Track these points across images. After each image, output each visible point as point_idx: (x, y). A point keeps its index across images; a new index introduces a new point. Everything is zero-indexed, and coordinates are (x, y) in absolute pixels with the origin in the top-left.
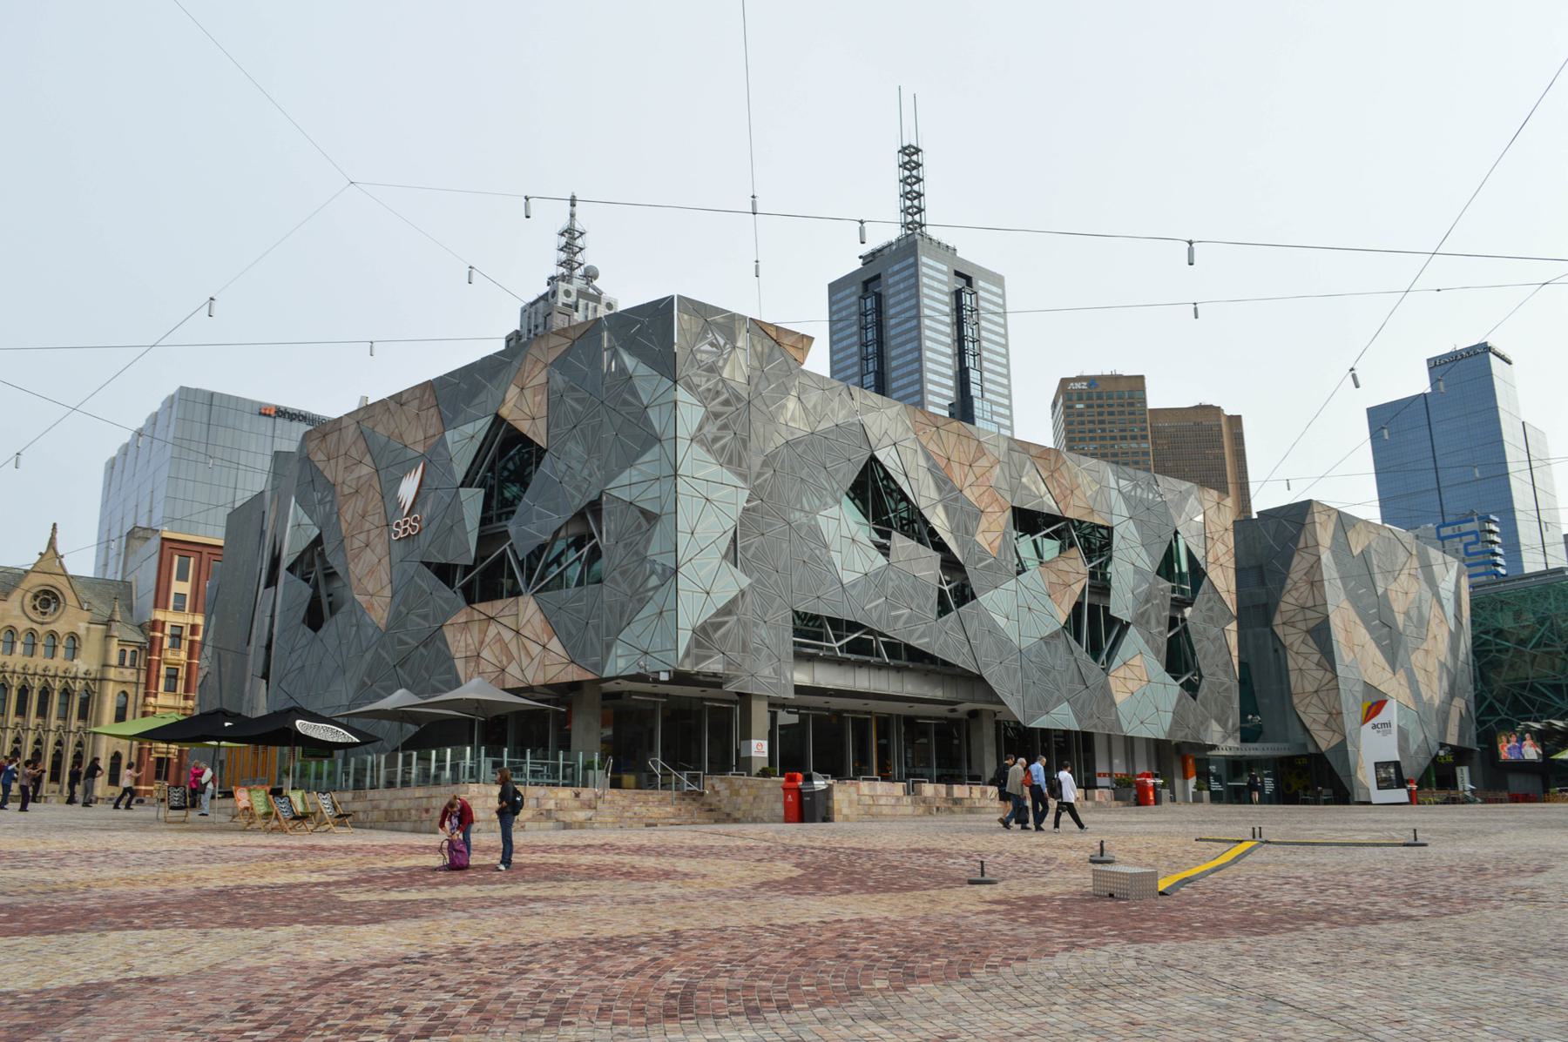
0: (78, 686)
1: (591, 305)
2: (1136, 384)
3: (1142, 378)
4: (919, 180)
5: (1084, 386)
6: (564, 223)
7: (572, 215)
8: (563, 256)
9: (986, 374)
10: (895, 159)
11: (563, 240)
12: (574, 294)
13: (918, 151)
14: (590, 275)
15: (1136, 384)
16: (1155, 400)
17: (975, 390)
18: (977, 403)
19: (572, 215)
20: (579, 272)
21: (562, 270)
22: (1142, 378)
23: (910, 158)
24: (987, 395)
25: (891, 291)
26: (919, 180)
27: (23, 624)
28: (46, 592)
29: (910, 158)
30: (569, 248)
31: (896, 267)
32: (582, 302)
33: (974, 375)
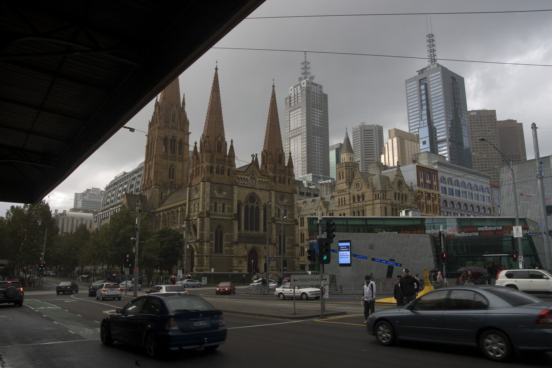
0: (360, 209)
2: (493, 113)
3: (495, 111)
4: (434, 45)
5: (475, 114)
7: (305, 57)
8: (303, 71)
11: (303, 66)
13: (433, 35)
15: (493, 113)
16: (500, 117)
19: (305, 57)
20: (308, 76)
21: (303, 76)
22: (495, 111)
25: (431, 83)
26: (434, 45)
27: (398, 191)
28: (399, 182)
30: (306, 67)
31: (433, 75)
32: (312, 86)
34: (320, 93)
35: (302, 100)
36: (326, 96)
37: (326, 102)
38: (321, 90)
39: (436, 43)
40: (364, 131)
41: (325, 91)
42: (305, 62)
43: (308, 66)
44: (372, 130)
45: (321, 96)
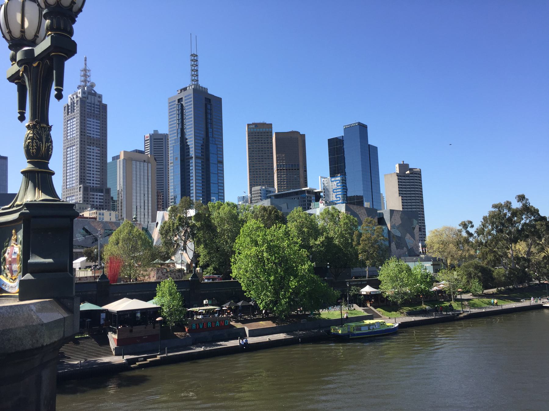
1: (93, 97)
6: (83, 66)
7: (86, 64)
8: (83, 78)
9: (215, 129)
10: (189, 58)
11: (82, 73)
12: (87, 93)
13: (197, 56)
14: (92, 86)
17: (210, 135)
18: (210, 139)
19: (86, 64)
22: (271, 124)
23: (194, 58)
24: (215, 136)
29: (194, 58)
30: (85, 75)
33: (210, 130)
34: (98, 104)
35: (77, 109)
36: (105, 106)
37: (105, 112)
38: (99, 99)
39: (200, 63)
40: (154, 139)
41: (104, 102)
42: (85, 70)
43: (88, 74)
44: (162, 139)
45: (99, 106)
